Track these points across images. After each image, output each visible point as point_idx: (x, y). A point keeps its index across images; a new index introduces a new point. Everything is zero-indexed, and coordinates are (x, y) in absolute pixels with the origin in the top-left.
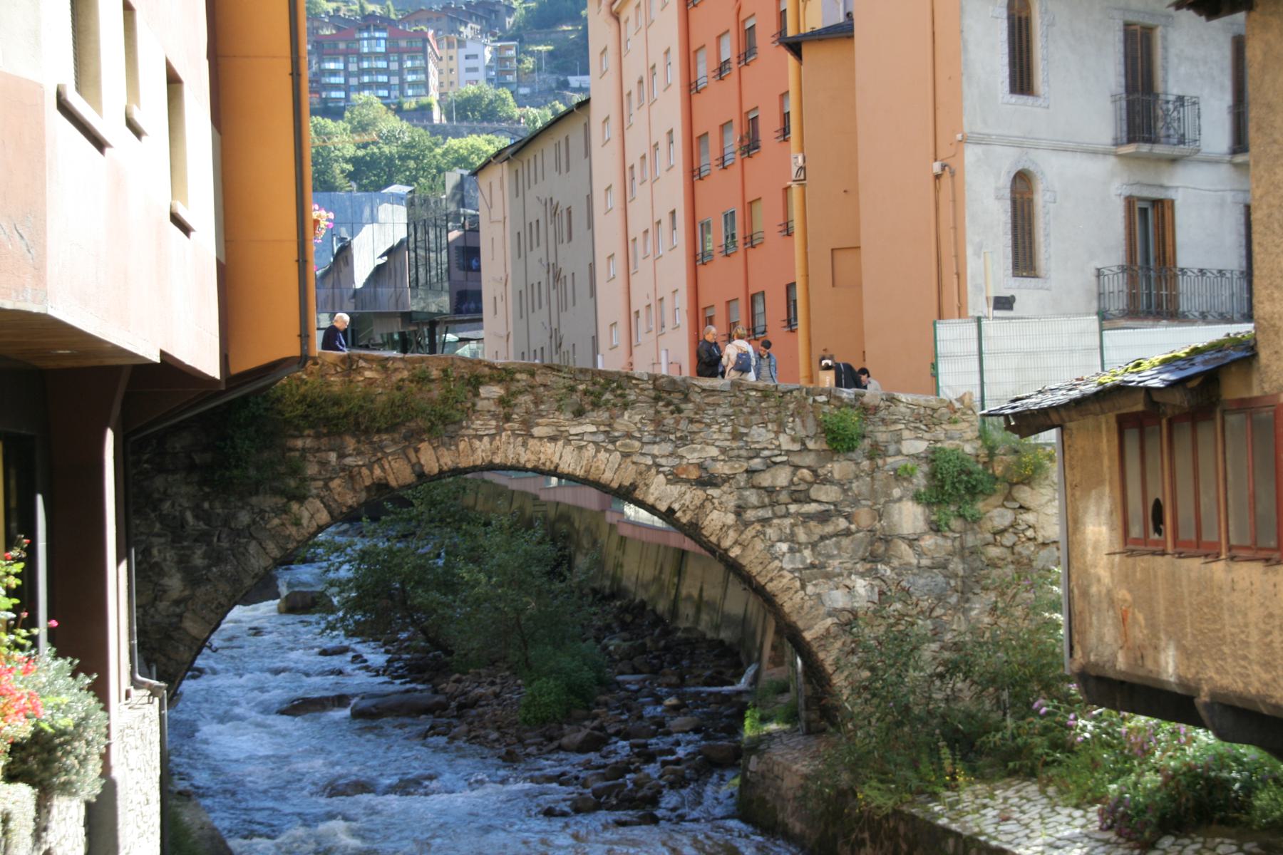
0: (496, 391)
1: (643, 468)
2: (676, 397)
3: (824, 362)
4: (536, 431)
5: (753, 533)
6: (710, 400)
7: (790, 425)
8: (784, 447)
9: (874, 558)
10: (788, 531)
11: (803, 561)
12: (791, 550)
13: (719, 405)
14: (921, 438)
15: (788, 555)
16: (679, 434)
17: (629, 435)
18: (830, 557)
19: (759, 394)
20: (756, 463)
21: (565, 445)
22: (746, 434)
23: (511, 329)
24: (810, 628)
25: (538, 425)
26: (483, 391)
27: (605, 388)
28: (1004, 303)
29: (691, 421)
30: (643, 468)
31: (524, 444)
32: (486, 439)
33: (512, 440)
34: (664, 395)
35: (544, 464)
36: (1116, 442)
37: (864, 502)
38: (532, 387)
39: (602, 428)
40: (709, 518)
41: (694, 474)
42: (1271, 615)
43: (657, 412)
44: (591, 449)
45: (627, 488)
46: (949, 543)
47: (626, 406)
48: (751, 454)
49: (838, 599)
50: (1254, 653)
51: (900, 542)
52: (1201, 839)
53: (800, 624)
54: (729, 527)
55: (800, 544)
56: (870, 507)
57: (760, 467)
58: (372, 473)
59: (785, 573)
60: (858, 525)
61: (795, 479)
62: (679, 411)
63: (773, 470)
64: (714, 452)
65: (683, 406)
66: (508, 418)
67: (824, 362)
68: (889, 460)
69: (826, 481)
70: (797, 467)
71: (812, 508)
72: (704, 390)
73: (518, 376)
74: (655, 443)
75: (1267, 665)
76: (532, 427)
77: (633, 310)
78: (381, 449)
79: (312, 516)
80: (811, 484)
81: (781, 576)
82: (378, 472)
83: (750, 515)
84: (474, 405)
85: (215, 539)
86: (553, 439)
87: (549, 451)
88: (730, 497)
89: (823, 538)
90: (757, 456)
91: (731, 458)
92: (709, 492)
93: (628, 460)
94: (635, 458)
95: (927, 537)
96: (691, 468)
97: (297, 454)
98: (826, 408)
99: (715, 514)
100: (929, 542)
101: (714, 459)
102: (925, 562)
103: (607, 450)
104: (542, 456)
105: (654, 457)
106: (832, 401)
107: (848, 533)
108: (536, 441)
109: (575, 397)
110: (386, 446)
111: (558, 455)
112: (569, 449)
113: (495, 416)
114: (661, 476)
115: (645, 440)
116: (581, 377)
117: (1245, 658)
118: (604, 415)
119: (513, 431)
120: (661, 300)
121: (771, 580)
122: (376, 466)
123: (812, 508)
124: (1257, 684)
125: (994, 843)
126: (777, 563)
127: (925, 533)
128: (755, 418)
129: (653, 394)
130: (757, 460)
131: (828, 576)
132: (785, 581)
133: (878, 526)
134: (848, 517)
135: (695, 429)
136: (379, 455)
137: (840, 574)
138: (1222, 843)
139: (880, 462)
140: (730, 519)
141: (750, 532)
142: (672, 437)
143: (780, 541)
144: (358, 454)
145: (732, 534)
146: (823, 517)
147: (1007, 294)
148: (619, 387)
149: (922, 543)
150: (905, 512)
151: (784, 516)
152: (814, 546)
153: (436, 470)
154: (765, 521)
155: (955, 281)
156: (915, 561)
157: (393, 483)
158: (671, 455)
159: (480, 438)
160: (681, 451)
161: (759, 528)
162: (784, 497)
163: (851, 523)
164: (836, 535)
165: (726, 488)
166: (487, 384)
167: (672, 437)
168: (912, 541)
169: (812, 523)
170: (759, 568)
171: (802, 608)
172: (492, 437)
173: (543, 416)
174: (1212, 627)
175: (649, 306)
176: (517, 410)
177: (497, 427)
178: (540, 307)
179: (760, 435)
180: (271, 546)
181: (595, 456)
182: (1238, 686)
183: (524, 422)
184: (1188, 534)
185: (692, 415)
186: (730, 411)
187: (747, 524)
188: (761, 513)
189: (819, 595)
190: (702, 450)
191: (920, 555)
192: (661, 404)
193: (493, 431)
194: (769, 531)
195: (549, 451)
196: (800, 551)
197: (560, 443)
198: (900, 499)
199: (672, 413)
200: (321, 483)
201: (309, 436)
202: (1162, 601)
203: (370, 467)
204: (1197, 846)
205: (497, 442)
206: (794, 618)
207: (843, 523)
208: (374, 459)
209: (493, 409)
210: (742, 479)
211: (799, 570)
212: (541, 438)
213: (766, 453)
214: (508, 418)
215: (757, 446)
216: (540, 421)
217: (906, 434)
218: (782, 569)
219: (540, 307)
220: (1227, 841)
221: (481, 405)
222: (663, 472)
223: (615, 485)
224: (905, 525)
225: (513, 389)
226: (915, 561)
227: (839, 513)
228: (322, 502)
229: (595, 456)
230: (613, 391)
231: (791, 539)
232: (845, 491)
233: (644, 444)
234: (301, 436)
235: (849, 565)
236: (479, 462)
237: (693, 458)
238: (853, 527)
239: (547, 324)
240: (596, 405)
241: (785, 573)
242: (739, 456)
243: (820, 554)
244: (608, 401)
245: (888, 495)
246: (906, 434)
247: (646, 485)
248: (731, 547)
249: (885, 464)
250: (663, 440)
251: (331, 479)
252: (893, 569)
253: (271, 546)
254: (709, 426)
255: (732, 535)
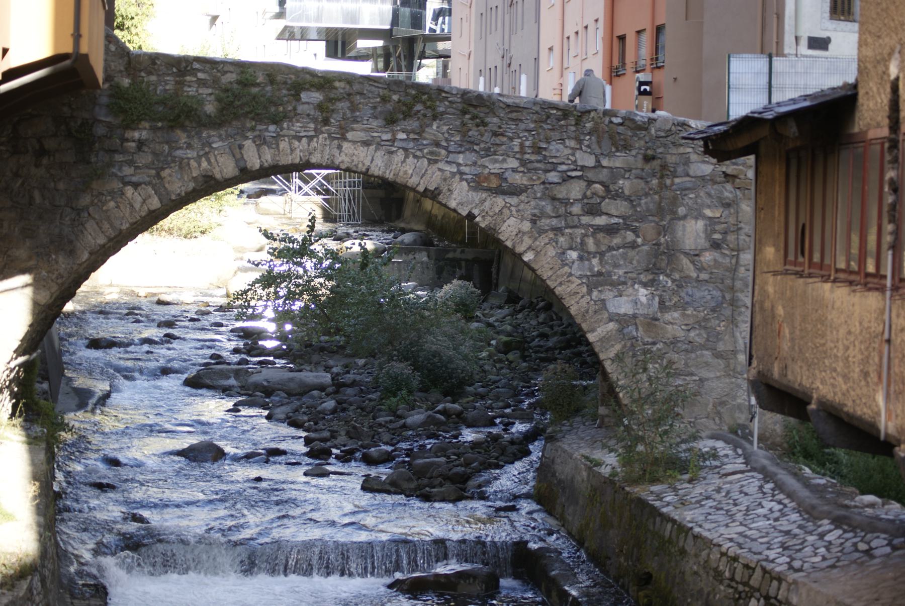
0: (316, 97)
1: (448, 174)
2: (480, 112)
3: (643, 88)
4: (349, 135)
5: (547, 241)
6: (514, 115)
7: (586, 143)
8: (580, 163)
9: (654, 269)
10: (579, 240)
11: (591, 269)
12: (581, 258)
13: (521, 120)
14: (708, 162)
15: (576, 263)
16: (482, 146)
17: (437, 144)
18: (616, 266)
19: (560, 113)
20: (553, 177)
21: (376, 150)
22: (545, 149)
23: (472, 48)
24: (593, 330)
25: (353, 129)
26: (304, 96)
27: (416, 99)
28: (819, 44)
29: (495, 134)
30: (448, 174)
31: (340, 147)
32: (304, 140)
33: (328, 142)
34: (471, 109)
35: (356, 166)
36: (784, 171)
37: (651, 218)
38: (349, 95)
39: (412, 136)
40: (506, 224)
41: (494, 183)
42: (849, 333)
43: (463, 124)
44: (401, 155)
45: (433, 192)
46: (728, 260)
47: (435, 118)
48: (549, 167)
49: (622, 306)
50: (840, 366)
51: (682, 256)
52: (863, 534)
53: (584, 326)
54: (524, 233)
55: (589, 253)
56: (657, 223)
57: (556, 180)
58: (200, 165)
59: (573, 279)
60: (644, 239)
61: (589, 193)
62: (484, 124)
63: (568, 184)
64: (513, 163)
65: (488, 120)
66: (326, 122)
67: (643, 88)
68: (677, 180)
69: (617, 195)
70: (590, 183)
71: (601, 221)
72: (508, 106)
73: (337, 84)
74: (459, 153)
75: (846, 377)
76: (347, 131)
77: (566, 35)
78: (209, 144)
79: (144, 201)
80: (603, 198)
81: (569, 281)
82: (204, 164)
83: (544, 223)
84: (295, 109)
85: (58, 217)
86: (366, 144)
87: (362, 155)
88: (527, 206)
89: (611, 249)
90: (554, 170)
91: (529, 170)
92: (507, 200)
93: (435, 167)
94: (441, 165)
95: (707, 254)
96: (492, 177)
97: (133, 144)
98: (621, 129)
99: (512, 221)
100: (708, 257)
101: (514, 170)
102: (704, 276)
103: (415, 157)
104: (354, 158)
105: (459, 165)
106: (627, 123)
107: (633, 246)
108: (350, 144)
109: (389, 106)
110: (213, 143)
111: (370, 158)
112: (379, 154)
113: (315, 120)
114: (464, 183)
115: (451, 149)
116: (394, 88)
117: (835, 370)
118: (413, 124)
119: (330, 134)
120: (586, 27)
121: (561, 284)
122: (203, 159)
123: (601, 221)
124: (840, 395)
125: (697, 530)
126: (566, 269)
127: (706, 250)
128: (556, 135)
129: (460, 106)
130: (553, 174)
131: (613, 284)
132: (573, 286)
133: (662, 240)
134: (635, 231)
135: (498, 142)
136: (207, 149)
137: (624, 283)
138: (878, 537)
139: (668, 182)
140: (526, 226)
141: (543, 240)
142: (476, 147)
143: (571, 249)
144: (187, 148)
145: (526, 238)
146: (611, 230)
147: (823, 35)
148: (430, 99)
149: (702, 259)
150: (688, 229)
151: (575, 227)
152: (602, 254)
153: (257, 166)
154: (557, 230)
155: (775, 20)
156: (694, 275)
157: (218, 176)
158: (475, 164)
159: (299, 139)
160: (485, 161)
161: (552, 236)
162: (576, 209)
163: (638, 236)
164: (624, 247)
165: (523, 197)
166: (308, 90)
167: (476, 147)
168: (694, 256)
169: (600, 236)
170: (550, 273)
171: (587, 312)
172: (310, 138)
173: (358, 122)
174: (823, 341)
175: (577, 33)
176: (334, 116)
177: (315, 130)
178: (496, 30)
179: (558, 151)
180: (106, 226)
181: (404, 162)
182: (830, 396)
183: (341, 127)
184: (817, 258)
185: (495, 129)
186: (532, 126)
187: (541, 232)
188: (554, 222)
189: (603, 301)
190: (504, 161)
191: (701, 269)
192: (467, 116)
193: (313, 133)
194: (562, 239)
195: (362, 155)
196: (589, 260)
197: (373, 147)
198: (684, 217)
199: (478, 126)
200: (154, 172)
201: (145, 129)
202: (798, 317)
203: (198, 159)
204: (859, 539)
205: (314, 144)
206: (578, 320)
207: (630, 236)
208: (202, 153)
209: (312, 113)
210: (539, 189)
211: (587, 276)
212: (354, 142)
213: (564, 167)
214: (326, 122)
215: (554, 160)
216: (355, 126)
217: (694, 157)
218: (571, 275)
219: (496, 30)
220: (883, 536)
221: (300, 108)
222: (466, 180)
223: (421, 189)
224: (687, 242)
225: (332, 96)
226: (694, 275)
227: (628, 227)
228: (154, 189)
229: (404, 162)
230: (424, 103)
231: (582, 247)
232: (634, 207)
233: (450, 152)
234: (139, 129)
235: (634, 275)
236: (297, 161)
237: (495, 168)
238: (639, 240)
239: (500, 45)
240: (407, 115)
241: (573, 279)
242: (536, 169)
243: (606, 263)
244: (419, 111)
245: (674, 213)
246: (694, 157)
247: (449, 190)
248: (525, 252)
249: (673, 184)
250: (467, 150)
251: (163, 169)
252: (674, 281)
253: (106, 226)
254: (511, 139)
255: (527, 241)
